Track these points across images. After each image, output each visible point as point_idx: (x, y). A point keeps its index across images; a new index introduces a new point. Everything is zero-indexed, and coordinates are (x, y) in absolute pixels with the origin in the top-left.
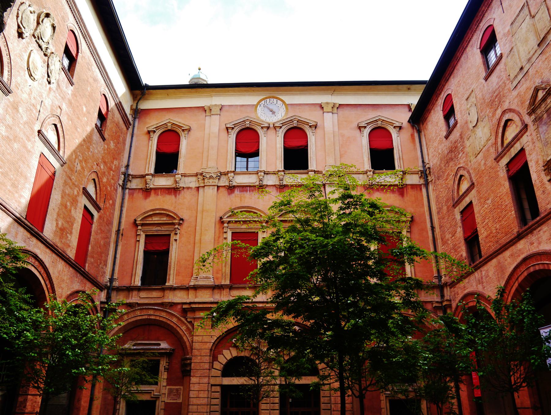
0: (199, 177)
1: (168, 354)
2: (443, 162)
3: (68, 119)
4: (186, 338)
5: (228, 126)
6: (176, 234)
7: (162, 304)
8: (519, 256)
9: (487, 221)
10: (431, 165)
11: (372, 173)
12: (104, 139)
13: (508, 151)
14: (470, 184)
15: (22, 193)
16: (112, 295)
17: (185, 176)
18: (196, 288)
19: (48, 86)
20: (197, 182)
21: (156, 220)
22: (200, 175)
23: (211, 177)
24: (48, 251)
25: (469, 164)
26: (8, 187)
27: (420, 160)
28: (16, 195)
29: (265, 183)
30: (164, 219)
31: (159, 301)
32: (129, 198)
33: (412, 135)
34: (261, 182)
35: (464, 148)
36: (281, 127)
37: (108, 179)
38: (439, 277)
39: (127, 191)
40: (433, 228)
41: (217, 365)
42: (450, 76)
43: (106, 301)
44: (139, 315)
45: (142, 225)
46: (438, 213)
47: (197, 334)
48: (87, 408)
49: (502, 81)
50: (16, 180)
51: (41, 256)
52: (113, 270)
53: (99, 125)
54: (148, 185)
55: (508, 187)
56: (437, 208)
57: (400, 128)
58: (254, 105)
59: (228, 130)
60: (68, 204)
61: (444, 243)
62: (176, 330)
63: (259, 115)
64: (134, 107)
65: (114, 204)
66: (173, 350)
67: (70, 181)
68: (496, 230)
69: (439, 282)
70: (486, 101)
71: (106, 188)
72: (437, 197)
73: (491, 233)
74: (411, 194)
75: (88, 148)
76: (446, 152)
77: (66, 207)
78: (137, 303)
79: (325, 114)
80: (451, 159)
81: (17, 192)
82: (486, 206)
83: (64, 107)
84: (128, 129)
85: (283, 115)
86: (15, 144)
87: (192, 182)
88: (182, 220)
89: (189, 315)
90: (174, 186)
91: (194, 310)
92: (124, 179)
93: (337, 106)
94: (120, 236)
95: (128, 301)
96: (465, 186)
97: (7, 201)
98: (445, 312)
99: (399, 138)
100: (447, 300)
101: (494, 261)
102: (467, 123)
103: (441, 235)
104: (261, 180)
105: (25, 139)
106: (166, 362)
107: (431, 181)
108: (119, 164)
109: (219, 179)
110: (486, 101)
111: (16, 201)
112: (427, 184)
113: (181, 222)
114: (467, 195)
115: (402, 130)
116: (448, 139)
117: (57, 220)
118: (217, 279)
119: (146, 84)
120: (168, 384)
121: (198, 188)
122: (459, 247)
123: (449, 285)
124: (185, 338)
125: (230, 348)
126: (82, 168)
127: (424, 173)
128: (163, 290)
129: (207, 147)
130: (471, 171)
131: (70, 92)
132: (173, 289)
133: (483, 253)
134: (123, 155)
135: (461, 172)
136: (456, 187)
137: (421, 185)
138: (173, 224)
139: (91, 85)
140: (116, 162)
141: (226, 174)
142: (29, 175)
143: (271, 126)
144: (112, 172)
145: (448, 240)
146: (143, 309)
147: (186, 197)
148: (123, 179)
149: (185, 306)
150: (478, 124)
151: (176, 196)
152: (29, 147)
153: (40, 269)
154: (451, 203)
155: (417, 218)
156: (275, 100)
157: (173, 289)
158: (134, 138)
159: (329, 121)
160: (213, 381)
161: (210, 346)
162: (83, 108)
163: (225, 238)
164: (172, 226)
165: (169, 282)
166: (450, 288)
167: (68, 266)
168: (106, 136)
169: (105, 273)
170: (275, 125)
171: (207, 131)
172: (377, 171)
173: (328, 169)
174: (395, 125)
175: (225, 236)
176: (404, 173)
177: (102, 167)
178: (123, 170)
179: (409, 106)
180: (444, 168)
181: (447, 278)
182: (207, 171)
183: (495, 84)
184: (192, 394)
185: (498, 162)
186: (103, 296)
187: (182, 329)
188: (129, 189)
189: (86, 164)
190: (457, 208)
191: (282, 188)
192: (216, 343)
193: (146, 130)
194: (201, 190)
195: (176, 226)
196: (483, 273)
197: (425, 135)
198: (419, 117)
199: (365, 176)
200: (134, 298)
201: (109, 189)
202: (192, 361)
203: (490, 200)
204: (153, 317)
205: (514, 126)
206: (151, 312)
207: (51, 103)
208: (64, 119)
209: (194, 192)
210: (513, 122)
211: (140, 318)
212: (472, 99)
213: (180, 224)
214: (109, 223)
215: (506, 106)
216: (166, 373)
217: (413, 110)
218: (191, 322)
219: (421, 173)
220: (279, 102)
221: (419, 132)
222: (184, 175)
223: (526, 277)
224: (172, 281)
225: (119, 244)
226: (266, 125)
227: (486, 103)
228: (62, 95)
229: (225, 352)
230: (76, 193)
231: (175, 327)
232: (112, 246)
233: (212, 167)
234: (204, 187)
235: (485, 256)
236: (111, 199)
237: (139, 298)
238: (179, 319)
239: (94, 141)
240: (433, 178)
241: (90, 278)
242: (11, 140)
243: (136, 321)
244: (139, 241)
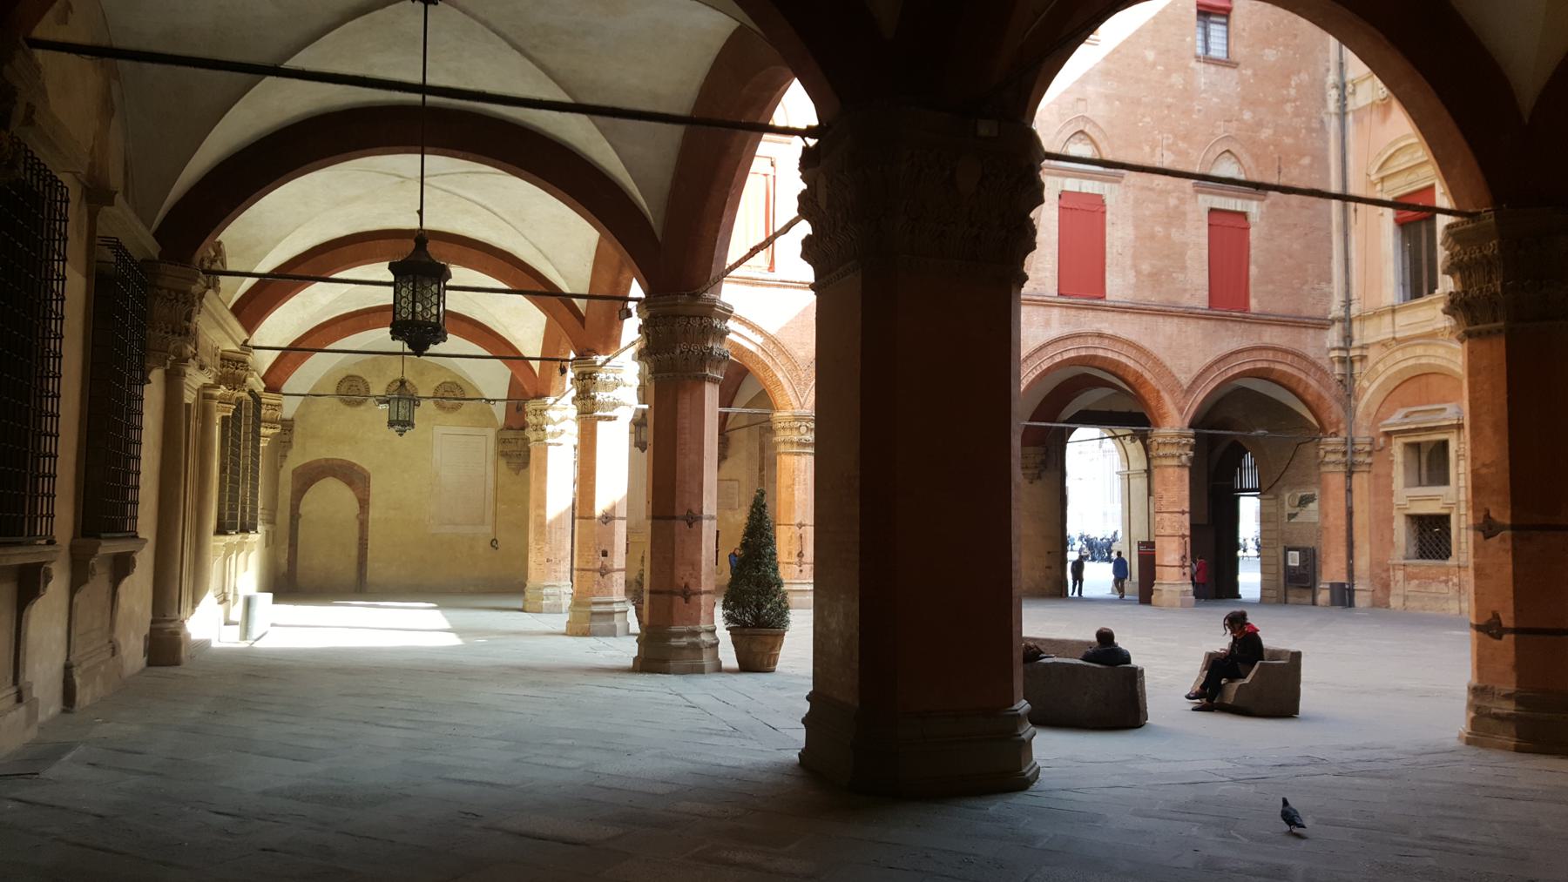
24: (1127, 316)
31: (1429, 329)
39: (1350, 118)
44: (1406, 360)
52: (1348, 283)
60: (1158, 229)
77: (1152, 237)
178: (1332, 78)
186: (1333, 336)
204: (1424, 361)
206: (1419, 351)
243: (1400, 371)
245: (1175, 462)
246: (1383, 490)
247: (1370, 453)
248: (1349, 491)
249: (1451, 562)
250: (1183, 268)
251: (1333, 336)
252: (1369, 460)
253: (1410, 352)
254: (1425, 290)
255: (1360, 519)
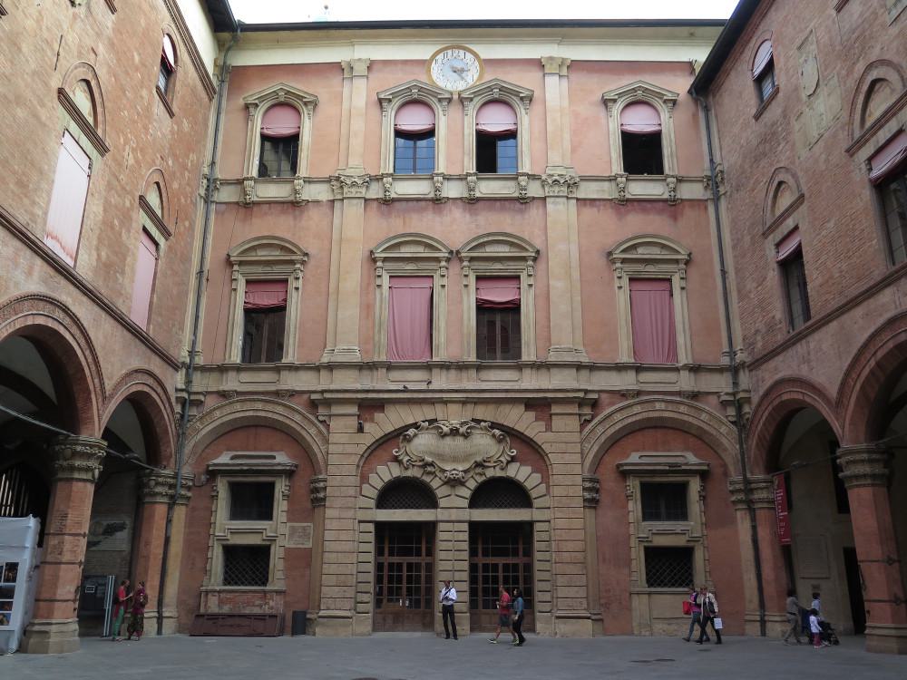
0: (334, 183)
1: (289, 474)
2: (748, 161)
3: (109, 73)
4: (317, 448)
5: (382, 96)
6: (297, 279)
7: (277, 393)
8: (881, 315)
9: (823, 258)
10: (726, 166)
11: (624, 179)
12: (171, 114)
13: (872, 136)
14: (797, 195)
15: (37, 200)
16: (194, 377)
17: (310, 182)
18: (331, 367)
19: (72, 10)
20: (330, 193)
21: (263, 255)
22: (336, 181)
23: (354, 184)
24: (85, 299)
25: (797, 160)
26: (12, 186)
27: (707, 159)
28: (26, 201)
29: (444, 194)
30: (276, 255)
31: (272, 388)
32: (216, 219)
33: (695, 116)
34: (438, 193)
35: (788, 134)
36: (471, 100)
37: (180, 184)
38: (732, 354)
40: (724, 272)
41: (366, 489)
42: (770, 7)
43: (184, 387)
44: (238, 411)
45: (241, 263)
46: (734, 247)
47: (335, 441)
48: (161, 556)
49: (871, 10)
50: (24, 174)
51: (73, 309)
53: (162, 83)
54: (248, 197)
55: (868, 198)
56: (732, 240)
57: (674, 102)
58: (426, 60)
59: (381, 103)
60: (116, 222)
61: (743, 296)
62: (300, 434)
63: (434, 77)
64: (221, 62)
65: (192, 228)
66: (296, 466)
67: (117, 183)
68: (841, 272)
69: (731, 362)
70: (837, 48)
71: (179, 200)
72: (734, 222)
73: (831, 277)
74: (689, 215)
75: (146, 129)
76: (755, 143)
77: (112, 227)
78: (235, 391)
79: (548, 79)
80: (765, 155)
81: (26, 196)
82: (824, 233)
83: (101, 49)
84: (211, 100)
85: (475, 78)
86: (19, 110)
87: (320, 192)
88: (306, 254)
89: (321, 410)
90: (292, 198)
91: (328, 403)
92: (208, 186)
93: (569, 62)
94: (204, 281)
95: (221, 388)
96: (785, 201)
97: (10, 210)
98: (739, 409)
99: (672, 120)
100: (744, 391)
101: (834, 324)
102: (796, 89)
103: (738, 284)
104: (437, 189)
105: (35, 102)
106: (286, 486)
107: (724, 194)
108: (198, 160)
109: (367, 187)
110: (837, 48)
111: (26, 211)
112: (716, 199)
113: (306, 259)
114: (789, 216)
115: (676, 106)
116: (760, 119)
117: (98, 249)
118: (367, 352)
119: (239, 21)
120: (289, 520)
121: (333, 201)
122: (770, 304)
123: (748, 367)
124: (315, 447)
125: (389, 463)
126: (137, 161)
127: (713, 182)
128: (278, 370)
129: (347, 130)
130: (800, 174)
131: (110, 24)
132: (293, 368)
133: (812, 312)
134: (205, 146)
135: (780, 177)
136: (770, 202)
137: (707, 200)
138: (292, 262)
139: (145, 15)
140: (193, 157)
141: (379, 178)
142: (46, 167)
143: (455, 97)
144: (186, 173)
145: (750, 292)
146: (246, 400)
147: (313, 218)
148: (205, 187)
149: (314, 397)
150: (818, 91)
151: (295, 218)
152: (44, 118)
153: (75, 330)
154: (759, 229)
155: (697, 257)
156: (462, 52)
157: (293, 368)
158: (223, 117)
159: (555, 90)
160: (361, 515)
161: (356, 459)
162: (133, 56)
163: (379, 286)
164: (292, 266)
165: (287, 357)
166: (751, 371)
167: (120, 327)
168: (175, 109)
169: (181, 341)
170: (462, 96)
171: (346, 105)
172: (632, 177)
173: (551, 173)
174: (665, 98)
175: (378, 282)
176: (680, 180)
177: (170, 163)
178: (206, 170)
179: (690, 64)
180: (749, 170)
181: (745, 354)
182: (348, 172)
183: (856, 16)
184: (328, 535)
185: (852, 156)
187: (310, 433)
188: (217, 203)
189: (143, 156)
190: (771, 237)
191: (472, 202)
192: (366, 455)
193: (241, 102)
194: (337, 204)
195: (298, 266)
196: (812, 345)
197: (716, 116)
198: (707, 83)
199: (613, 184)
200: (232, 383)
201: (183, 200)
202: (328, 484)
203: (832, 222)
205: (888, 90)
206: (259, 406)
207: (77, 41)
208: (102, 72)
209: (325, 209)
210: (885, 83)
211: (242, 415)
212: (812, 48)
213: (303, 263)
214: (186, 259)
215: (874, 55)
216: (285, 502)
217: (697, 71)
218: (325, 421)
219: (709, 180)
220: (469, 56)
221: (707, 109)
222: (308, 181)
223: (891, 351)
224: (291, 355)
225: (202, 295)
226: (447, 96)
227: (836, 53)
228: (97, 30)
229: (382, 469)
230: (128, 204)
231: (298, 429)
232: (192, 297)
233: (356, 166)
234: (342, 200)
235: (818, 317)
236: (186, 219)
237: (238, 384)
238: (306, 418)
239: (156, 117)
240: (728, 188)
241: (157, 349)
242: (10, 102)
244: (235, 290)
245: (89, 476)
246: (201, 524)
247: (189, 488)
248: (169, 521)
249: (268, 588)
250: (123, 273)
251: (178, 379)
252: (189, 494)
253: (248, 406)
254: (263, 357)
255: (176, 547)
